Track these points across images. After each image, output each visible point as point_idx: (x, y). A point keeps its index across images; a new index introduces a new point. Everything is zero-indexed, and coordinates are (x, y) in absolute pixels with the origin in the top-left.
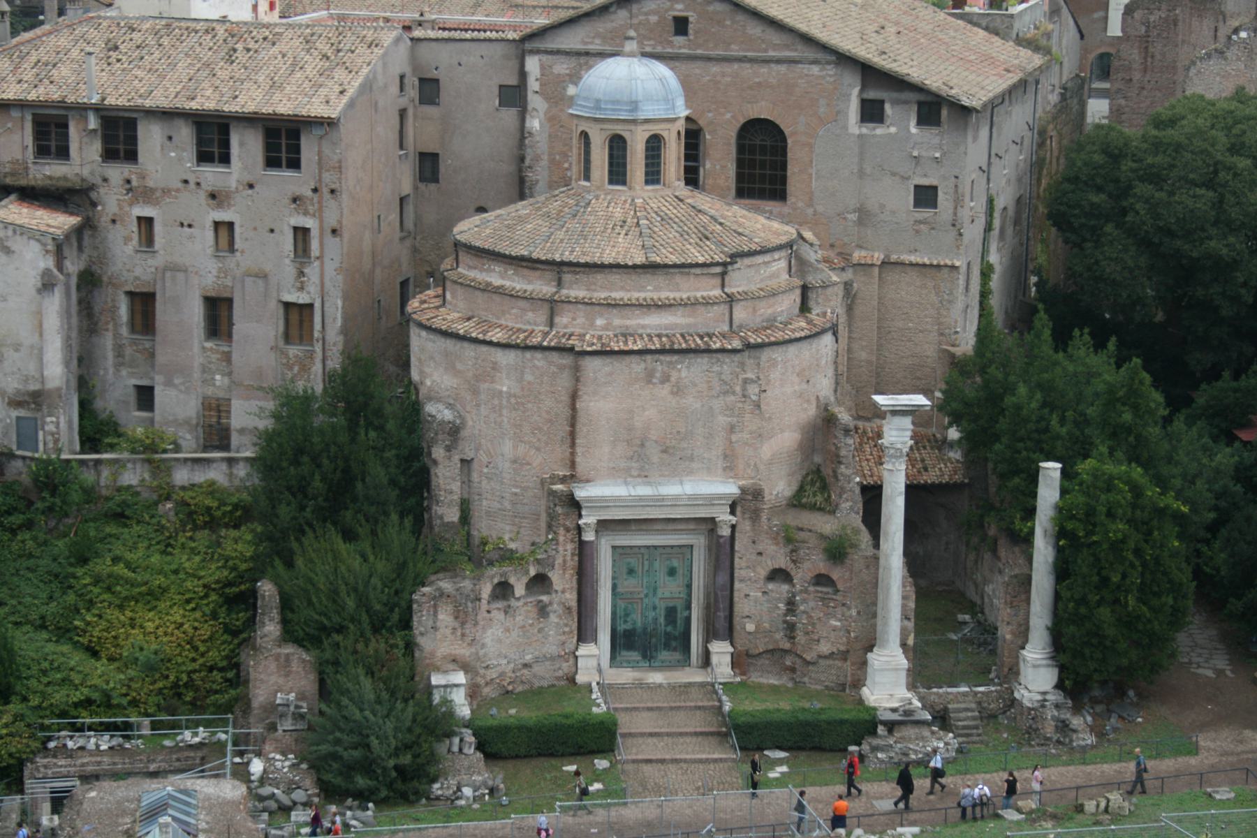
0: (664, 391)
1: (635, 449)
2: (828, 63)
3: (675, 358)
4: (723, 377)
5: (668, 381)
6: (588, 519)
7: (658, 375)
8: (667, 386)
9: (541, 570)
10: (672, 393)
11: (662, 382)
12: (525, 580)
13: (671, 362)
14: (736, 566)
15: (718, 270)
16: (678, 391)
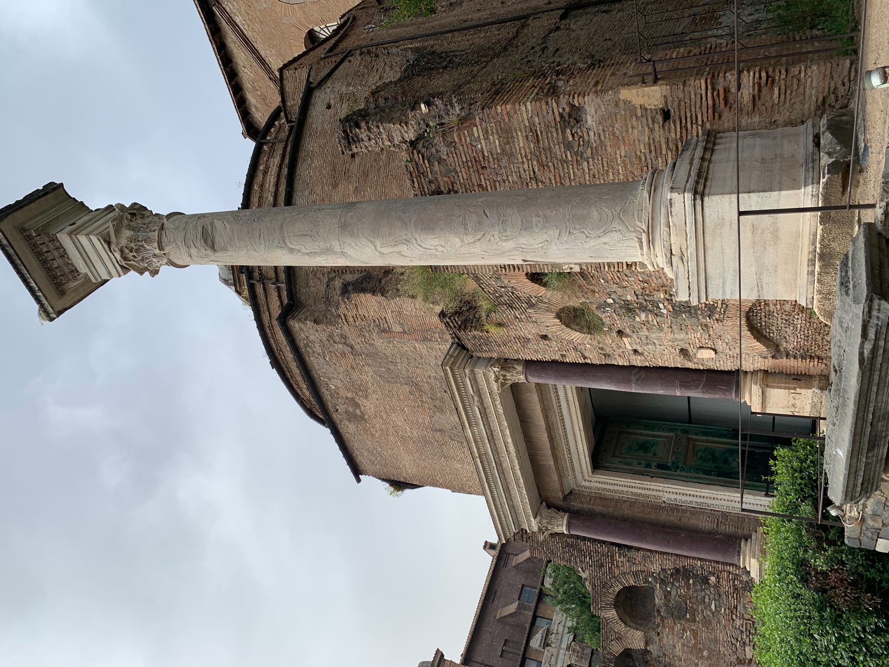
0: (368, 406)
1: (447, 438)
2: (224, 11)
3: (323, 390)
4: (324, 339)
5: (353, 399)
6: (533, 525)
7: (351, 409)
8: (361, 401)
9: (611, 598)
10: (366, 397)
11: (357, 405)
12: (621, 627)
13: (332, 396)
14: (581, 361)
15: (259, 289)
16: (362, 390)
